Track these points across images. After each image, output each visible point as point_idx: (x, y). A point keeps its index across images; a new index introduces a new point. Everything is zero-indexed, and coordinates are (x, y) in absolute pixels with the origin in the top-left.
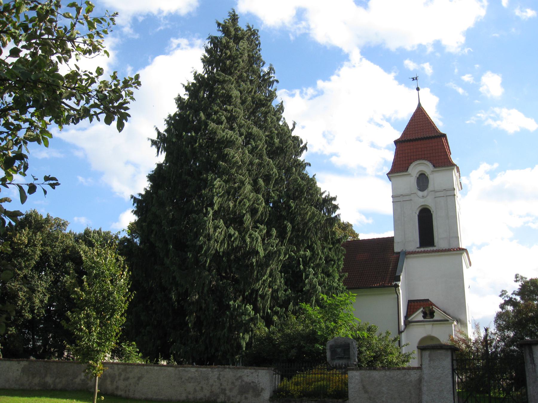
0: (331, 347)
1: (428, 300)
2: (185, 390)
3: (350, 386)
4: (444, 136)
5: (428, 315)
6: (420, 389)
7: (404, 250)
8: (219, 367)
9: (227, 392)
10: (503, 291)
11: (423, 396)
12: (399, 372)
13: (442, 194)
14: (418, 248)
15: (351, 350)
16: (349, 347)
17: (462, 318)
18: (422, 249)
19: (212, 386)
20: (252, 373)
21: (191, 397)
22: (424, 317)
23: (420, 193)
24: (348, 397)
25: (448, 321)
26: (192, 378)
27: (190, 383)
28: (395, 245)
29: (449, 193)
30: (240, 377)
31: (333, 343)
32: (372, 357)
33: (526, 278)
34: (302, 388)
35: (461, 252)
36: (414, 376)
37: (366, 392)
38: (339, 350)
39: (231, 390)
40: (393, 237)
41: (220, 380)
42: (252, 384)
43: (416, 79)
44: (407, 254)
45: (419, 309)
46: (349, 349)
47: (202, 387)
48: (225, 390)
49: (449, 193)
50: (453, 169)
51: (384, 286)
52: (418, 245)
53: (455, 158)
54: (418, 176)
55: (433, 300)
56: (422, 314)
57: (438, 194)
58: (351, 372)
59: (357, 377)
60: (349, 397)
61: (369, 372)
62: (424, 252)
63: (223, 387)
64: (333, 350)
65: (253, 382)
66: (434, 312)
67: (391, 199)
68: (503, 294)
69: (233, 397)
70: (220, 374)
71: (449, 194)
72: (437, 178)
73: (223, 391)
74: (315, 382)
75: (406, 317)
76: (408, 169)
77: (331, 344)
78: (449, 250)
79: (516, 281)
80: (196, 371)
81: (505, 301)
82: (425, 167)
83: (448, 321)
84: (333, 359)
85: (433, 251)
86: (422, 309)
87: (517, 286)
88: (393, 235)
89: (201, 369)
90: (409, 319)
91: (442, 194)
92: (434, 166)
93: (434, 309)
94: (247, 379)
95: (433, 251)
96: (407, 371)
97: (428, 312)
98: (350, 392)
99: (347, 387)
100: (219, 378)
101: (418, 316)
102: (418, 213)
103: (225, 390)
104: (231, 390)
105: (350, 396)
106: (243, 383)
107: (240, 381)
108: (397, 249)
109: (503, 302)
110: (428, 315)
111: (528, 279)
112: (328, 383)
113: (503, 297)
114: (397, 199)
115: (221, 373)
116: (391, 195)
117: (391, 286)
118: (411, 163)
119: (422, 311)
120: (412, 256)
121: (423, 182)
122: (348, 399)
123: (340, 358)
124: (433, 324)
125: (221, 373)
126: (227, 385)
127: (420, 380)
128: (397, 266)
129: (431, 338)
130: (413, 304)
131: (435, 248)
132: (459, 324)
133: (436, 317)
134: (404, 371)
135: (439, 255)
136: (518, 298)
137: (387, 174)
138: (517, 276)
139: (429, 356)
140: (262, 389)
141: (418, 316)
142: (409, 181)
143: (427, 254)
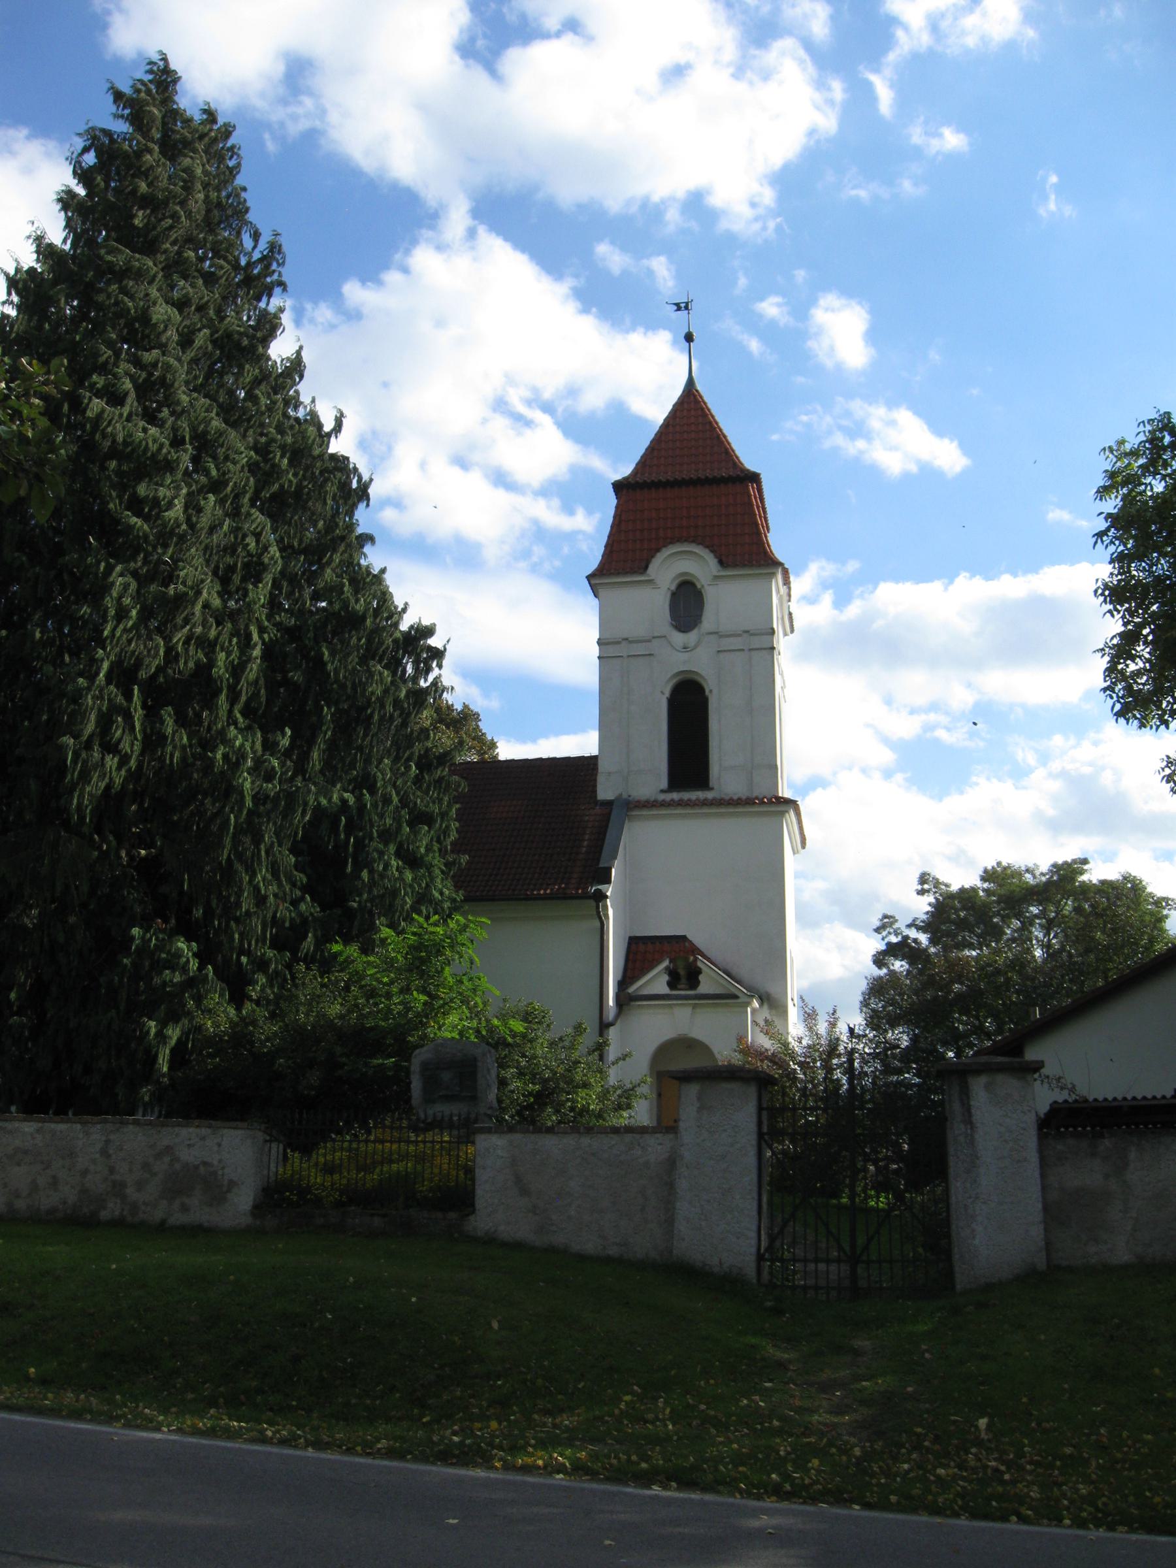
0: (425, 1066)
1: (684, 938)
2: (5, 1185)
3: (481, 1176)
4: (755, 478)
5: (683, 981)
6: (671, 1186)
7: (625, 796)
8: (106, 1121)
9: (129, 1191)
10: (885, 916)
11: (678, 1205)
12: (615, 1139)
13: (735, 643)
14: (662, 791)
17: (773, 990)
18: (675, 796)
19: (85, 1172)
20: (203, 1138)
21: (20, 1204)
22: (672, 985)
23: (678, 638)
24: (473, 1205)
25: (736, 997)
26: (26, 1152)
27: (19, 1165)
28: (601, 779)
29: (756, 642)
30: (169, 1149)
32: (531, 1094)
33: (947, 886)
34: (344, 1181)
35: (781, 808)
36: (656, 1148)
37: (524, 1191)
38: (446, 1076)
39: (140, 1185)
40: (595, 758)
41: (109, 1156)
42: (202, 1169)
43: (686, 308)
44: (632, 806)
45: (659, 962)
47: (54, 1177)
48: (123, 1185)
49: (756, 642)
50: (773, 574)
51: (564, 897)
52: (664, 784)
53: (778, 542)
54: (673, 588)
55: (698, 939)
56: (666, 978)
57: (728, 643)
58: (483, 1136)
59: (499, 1152)
60: (477, 1206)
61: (533, 1137)
62: (681, 804)
63: (118, 1177)
64: (431, 1072)
65: (205, 1164)
66: (699, 971)
67: (595, 650)
68: (886, 923)
69: (144, 1203)
70: (107, 1142)
71: (758, 644)
72: (725, 598)
73: (118, 1188)
74: (382, 1163)
75: (622, 985)
76: (646, 567)
78: (749, 802)
79: (921, 892)
80: (38, 1131)
81: (889, 944)
82: (698, 564)
83: (736, 997)
84: (428, 1099)
85: (705, 803)
86: (666, 963)
87: (922, 906)
88: (594, 751)
89: (53, 1126)
90: (631, 990)
91: (735, 643)
92: (721, 562)
93: (699, 964)
94: (187, 1156)
95: (705, 803)
96: (638, 1136)
97: (682, 972)
98: (479, 1192)
99: (473, 1180)
100: (104, 1153)
101: (656, 981)
102: (667, 693)
103: (123, 1185)
104: (140, 1185)
105: (480, 1203)
106: (178, 1166)
107: (167, 1159)
108: (605, 792)
109: (882, 946)
110: (683, 981)
111: (955, 888)
112: (419, 1168)
113: (884, 933)
114: (612, 651)
115: (112, 1137)
116: (596, 635)
117: (586, 896)
118: (658, 550)
119: (667, 968)
120: (645, 812)
121: (687, 604)
122: (474, 1212)
123: (450, 1098)
124: (695, 1006)
125: (112, 1137)
126: (131, 1171)
127: (672, 1163)
128: (603, 840)
129: (687, 1044)
130: (642, 947)
131: (709, 795)
132: (766, 1006)
133: (705, 987)
134: (628, 1138)
135: (722, 815)
136: (923, 938)
137: (589, 578)
138: (923, 878)
139: (699, 1099)
140: (232, 1184)
141: (656, 981)
142: (649, 600)
143: (689, 811)
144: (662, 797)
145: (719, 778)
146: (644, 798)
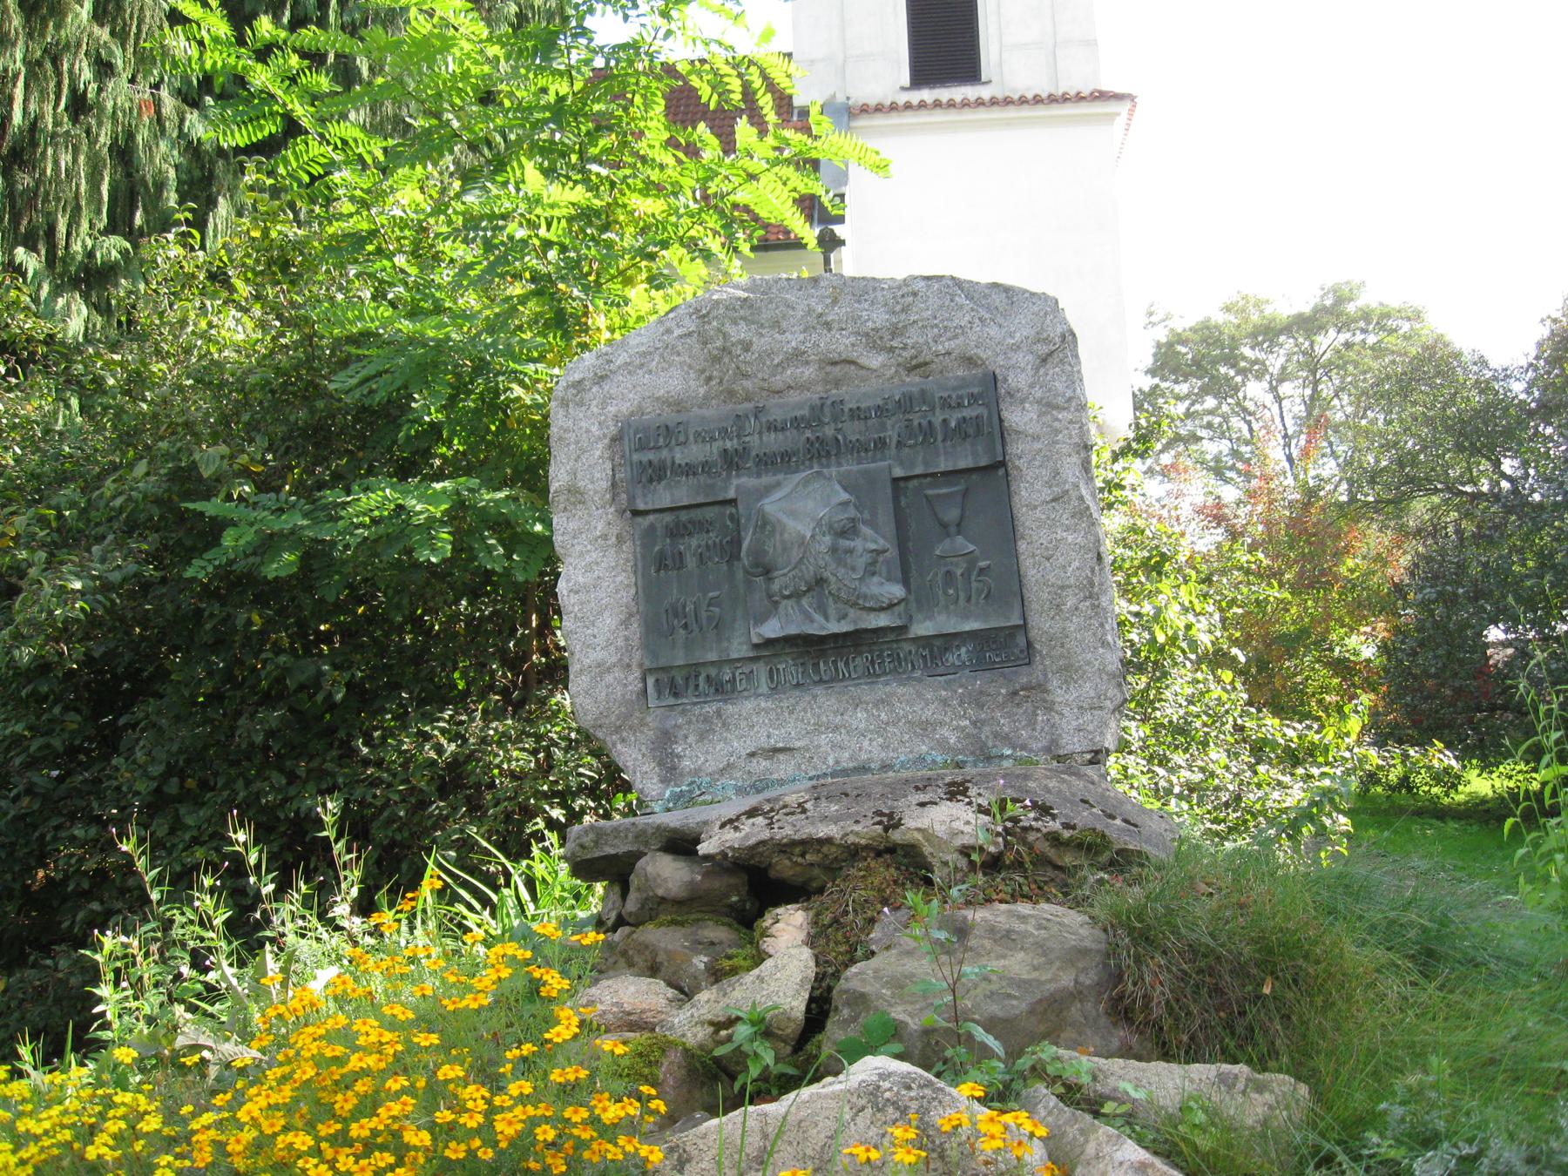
0: (646, 452)
7: (841, 98)
14: (903, 89)
15: (1029, 491)
16: (1001, 433)
18: (927, 95)
31: (674, 381)
35: (1111, 107)
38: (801, 509)
46: (997, 471)
52: (905, 78)
62: (937, 104)
77: (628, 397)
78: (1052, 100)
84: (682, 674)
85: (980, 103)
95: (980, 103)
123: (818, 656)
131: (985, 92)
135: (1008, 124)
144: (902, 98)
145: (1001, 65)
146: (873, 102)
